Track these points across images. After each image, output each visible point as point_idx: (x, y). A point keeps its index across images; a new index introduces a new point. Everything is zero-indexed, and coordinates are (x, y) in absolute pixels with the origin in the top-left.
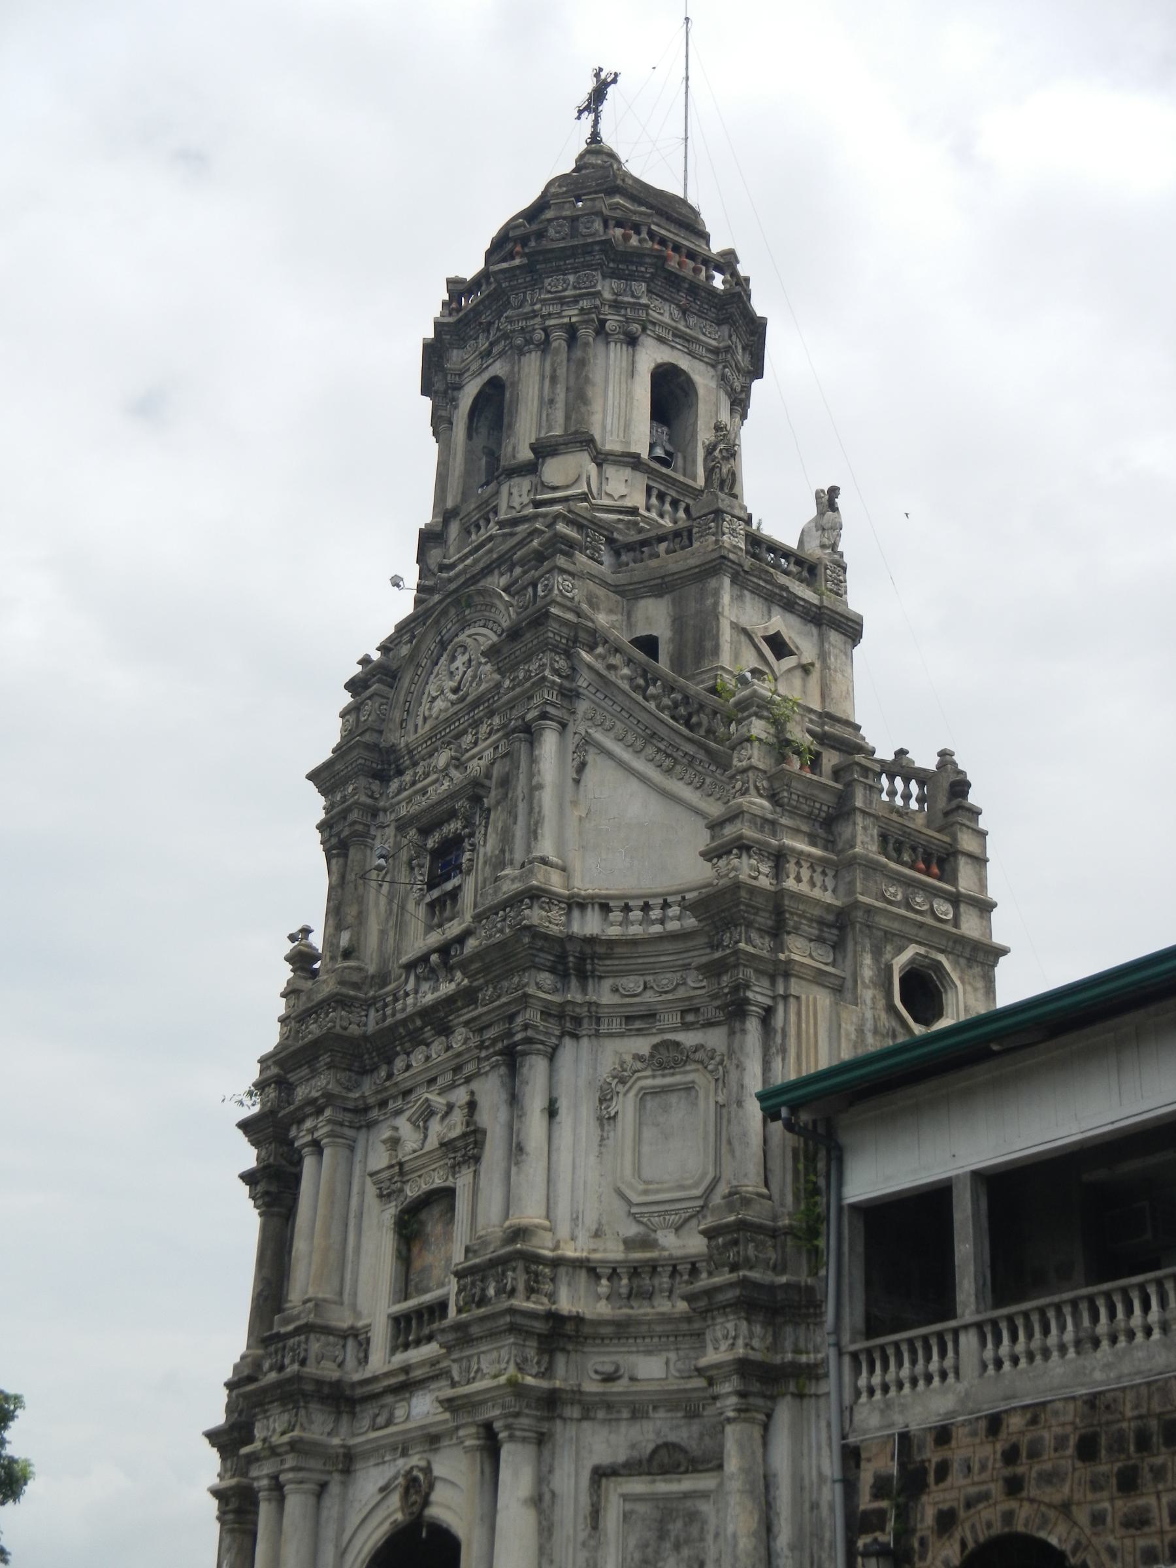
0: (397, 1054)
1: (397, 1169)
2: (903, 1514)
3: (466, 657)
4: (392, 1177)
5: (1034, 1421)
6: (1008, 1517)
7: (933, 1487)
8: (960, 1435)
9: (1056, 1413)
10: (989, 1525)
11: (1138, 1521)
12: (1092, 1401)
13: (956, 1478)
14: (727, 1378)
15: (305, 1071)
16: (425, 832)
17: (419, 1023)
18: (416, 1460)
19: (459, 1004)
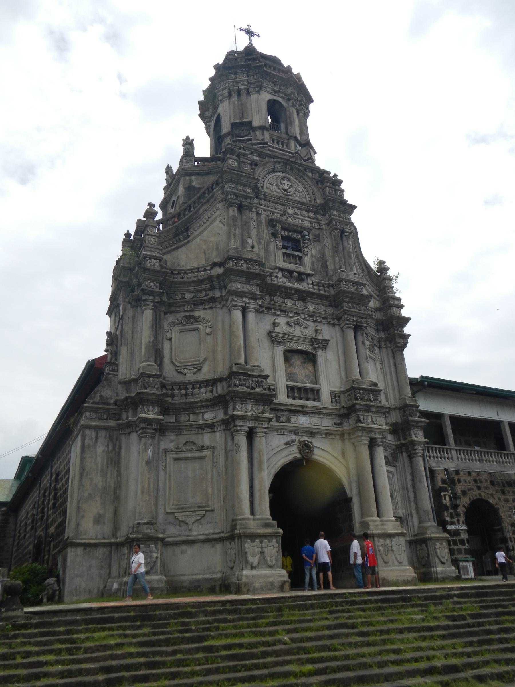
0: (276, 295)
1: (287, 336)
2: (452, 489)
3: (290, 184)
4: (283, 337)
5: (478, 475)
6: (480, 495)
7: (457, 484)
8: (461, 473)
9: (483, 474)
10: (476, 496)
11: (507, 501)
12: (490, 473)
13: (463, 483)
14: (420, 445)
15: (243, 279)
16: (283, 229)
17: (293, 292)
18: (305, 438)
19: (315, 297)
